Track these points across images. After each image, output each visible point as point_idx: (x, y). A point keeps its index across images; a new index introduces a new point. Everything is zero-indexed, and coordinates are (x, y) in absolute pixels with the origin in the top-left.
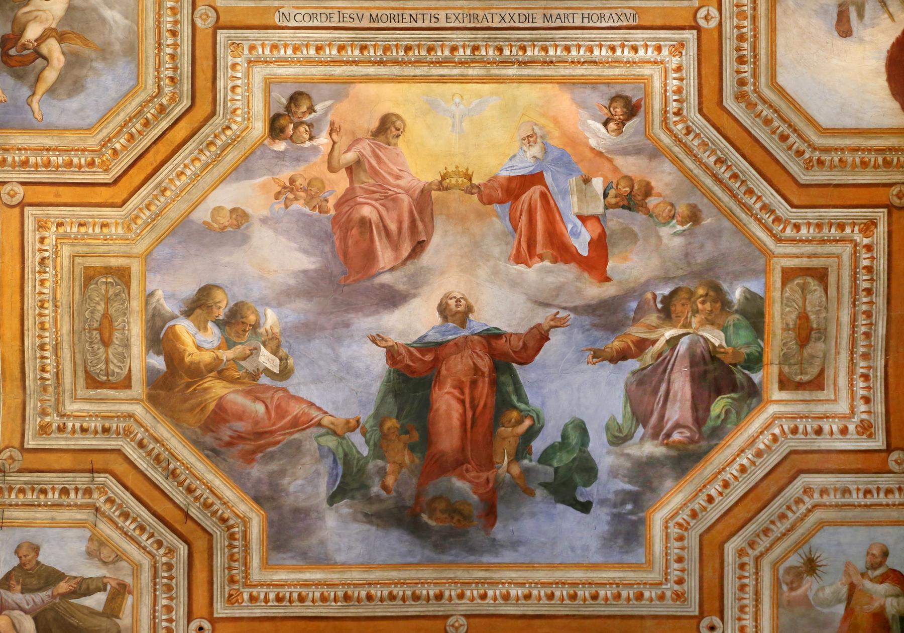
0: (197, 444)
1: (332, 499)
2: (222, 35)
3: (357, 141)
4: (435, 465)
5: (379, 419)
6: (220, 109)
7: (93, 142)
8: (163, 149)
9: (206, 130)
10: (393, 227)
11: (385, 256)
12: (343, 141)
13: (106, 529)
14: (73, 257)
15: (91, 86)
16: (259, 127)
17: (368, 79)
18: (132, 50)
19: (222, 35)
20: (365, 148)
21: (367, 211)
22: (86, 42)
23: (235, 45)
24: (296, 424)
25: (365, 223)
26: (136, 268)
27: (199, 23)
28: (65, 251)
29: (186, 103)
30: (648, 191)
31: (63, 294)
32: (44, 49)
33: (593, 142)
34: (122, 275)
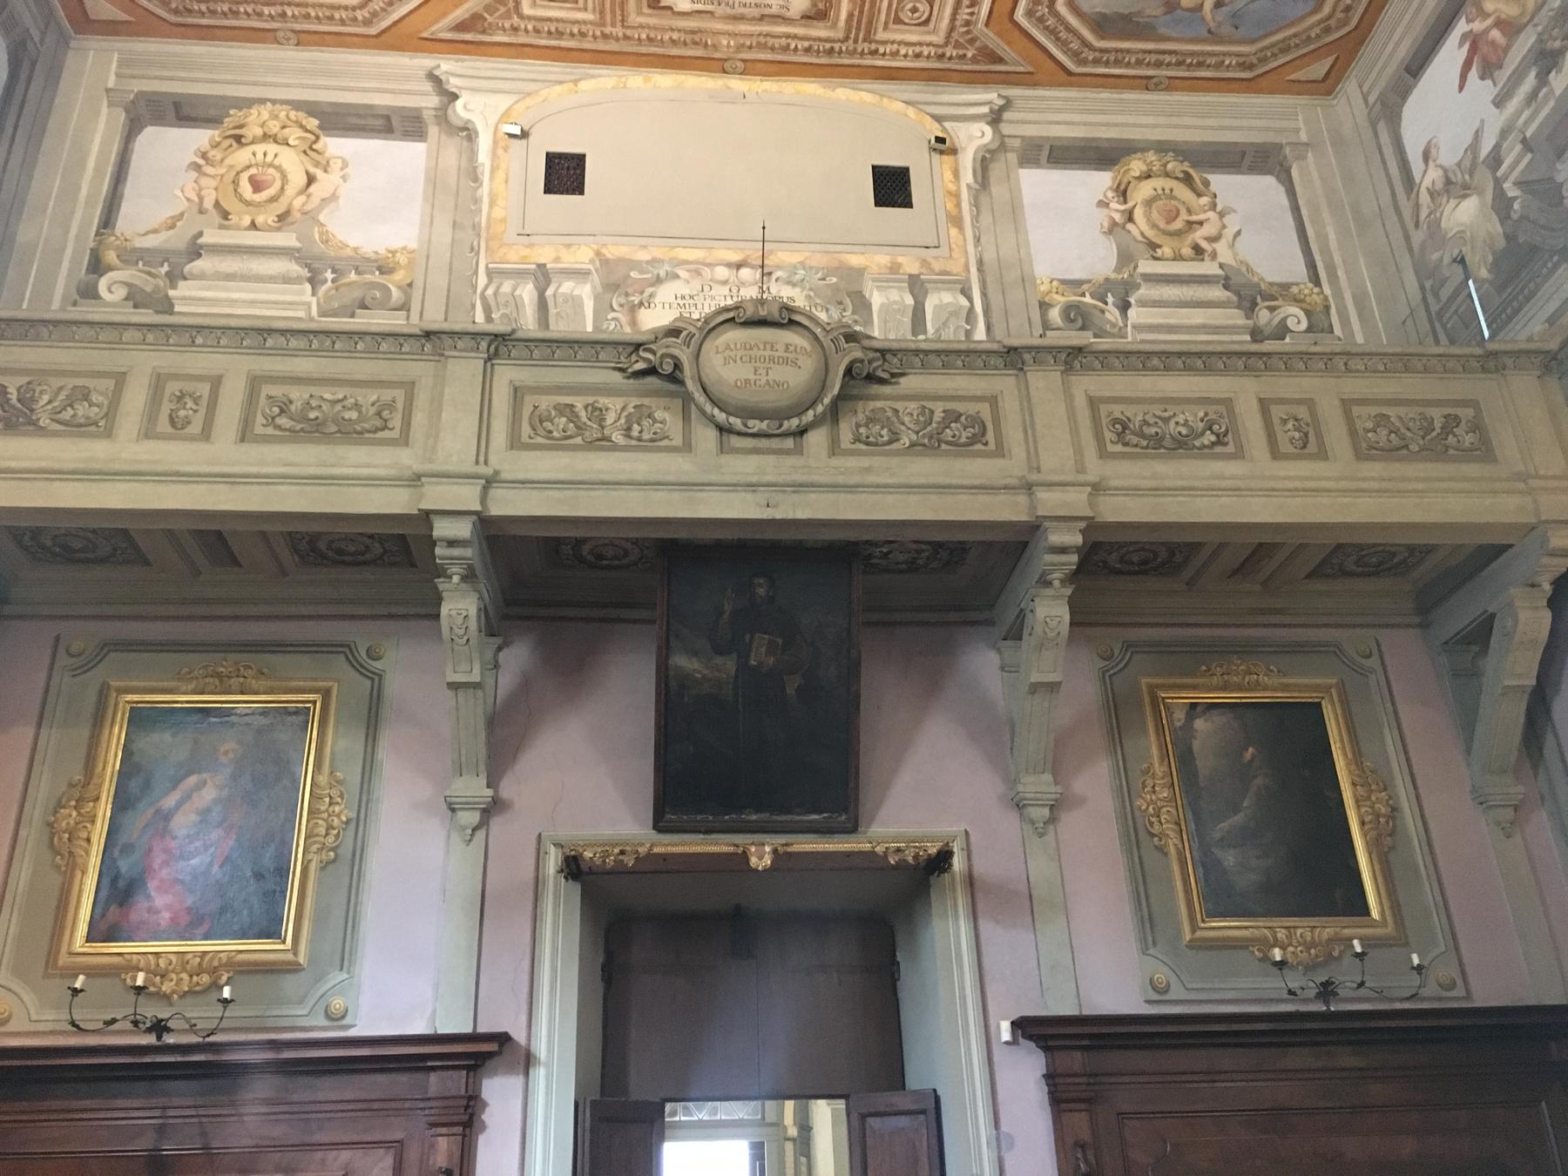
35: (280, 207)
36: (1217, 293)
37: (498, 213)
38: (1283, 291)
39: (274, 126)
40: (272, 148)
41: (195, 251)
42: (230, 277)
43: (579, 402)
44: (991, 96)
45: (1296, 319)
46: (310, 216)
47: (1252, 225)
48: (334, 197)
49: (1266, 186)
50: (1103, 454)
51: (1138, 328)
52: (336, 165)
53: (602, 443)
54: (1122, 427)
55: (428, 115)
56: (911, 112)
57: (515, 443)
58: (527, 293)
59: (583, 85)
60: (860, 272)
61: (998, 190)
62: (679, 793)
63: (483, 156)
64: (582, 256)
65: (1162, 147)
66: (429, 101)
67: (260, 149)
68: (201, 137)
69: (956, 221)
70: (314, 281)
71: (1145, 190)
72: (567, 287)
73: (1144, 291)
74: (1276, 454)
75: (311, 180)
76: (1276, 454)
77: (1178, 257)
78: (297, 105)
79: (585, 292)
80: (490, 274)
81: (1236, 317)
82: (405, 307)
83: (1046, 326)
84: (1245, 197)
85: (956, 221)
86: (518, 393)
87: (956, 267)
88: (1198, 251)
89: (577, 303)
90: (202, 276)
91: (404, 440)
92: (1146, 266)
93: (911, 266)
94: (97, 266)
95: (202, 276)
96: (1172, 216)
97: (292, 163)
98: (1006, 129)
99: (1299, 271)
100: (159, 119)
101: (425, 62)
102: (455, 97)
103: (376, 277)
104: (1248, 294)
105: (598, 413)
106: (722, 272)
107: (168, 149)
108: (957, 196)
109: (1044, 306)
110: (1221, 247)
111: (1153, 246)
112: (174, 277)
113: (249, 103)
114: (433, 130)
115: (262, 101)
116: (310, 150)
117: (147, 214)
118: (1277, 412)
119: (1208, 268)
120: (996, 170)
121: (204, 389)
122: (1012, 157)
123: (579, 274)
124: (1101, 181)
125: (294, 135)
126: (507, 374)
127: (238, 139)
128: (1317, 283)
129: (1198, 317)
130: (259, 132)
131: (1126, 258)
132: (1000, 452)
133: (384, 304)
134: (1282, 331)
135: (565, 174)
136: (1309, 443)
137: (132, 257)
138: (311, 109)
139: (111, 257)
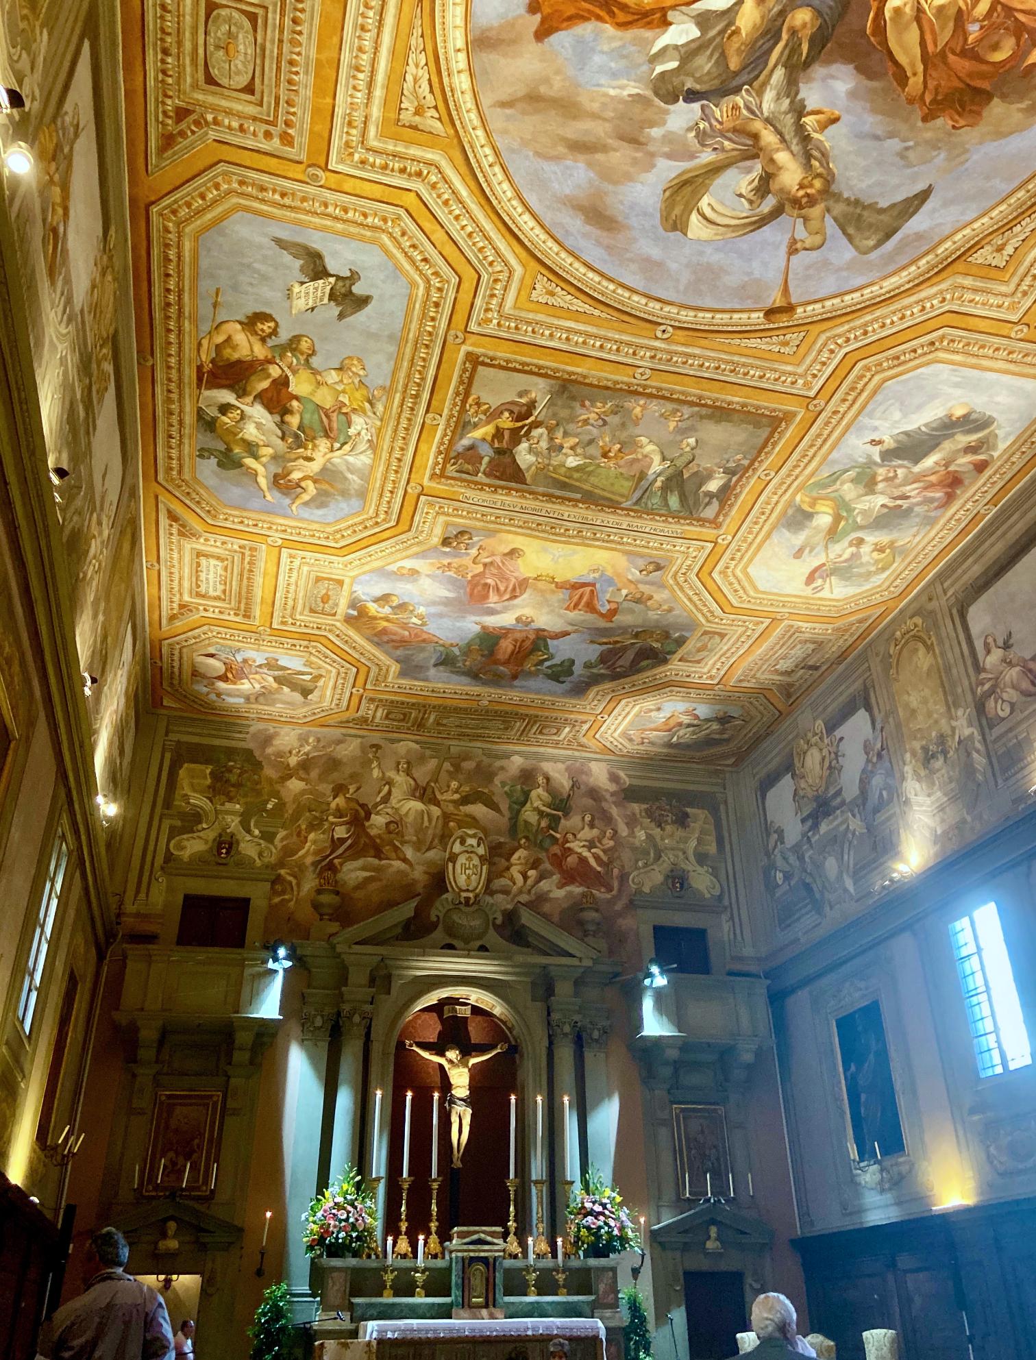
0: (372, 641)
1: (435, 665)
2: (423, 498)
3: (493, 555)
4: (497, 662)
5: (469, 645)
6: (414, 529)
7: (330, 530)
8: (373, 539)
9: (403, 536)
10: (502, 589)
11: (493, 597)
12: (484, 554)
13: (313, 659)
14: (309, 572)
15: (332, 505)
16: (436, 540)
17: (509, 532)
18: (362, 494)
19: (423, 498)
20: (498, 559)
21: (489, 581)
22: (332, 486)
23: (431, 504)
24: (424, 641)
25: (487, 586)
26: (347, 581)
27: (409, 490)
28: (305, 569)
29: (393, 523)
30: (650, 598)
31: (302, 583)
32: (303, 484)
33: (630, 577)
34: (340, 583)
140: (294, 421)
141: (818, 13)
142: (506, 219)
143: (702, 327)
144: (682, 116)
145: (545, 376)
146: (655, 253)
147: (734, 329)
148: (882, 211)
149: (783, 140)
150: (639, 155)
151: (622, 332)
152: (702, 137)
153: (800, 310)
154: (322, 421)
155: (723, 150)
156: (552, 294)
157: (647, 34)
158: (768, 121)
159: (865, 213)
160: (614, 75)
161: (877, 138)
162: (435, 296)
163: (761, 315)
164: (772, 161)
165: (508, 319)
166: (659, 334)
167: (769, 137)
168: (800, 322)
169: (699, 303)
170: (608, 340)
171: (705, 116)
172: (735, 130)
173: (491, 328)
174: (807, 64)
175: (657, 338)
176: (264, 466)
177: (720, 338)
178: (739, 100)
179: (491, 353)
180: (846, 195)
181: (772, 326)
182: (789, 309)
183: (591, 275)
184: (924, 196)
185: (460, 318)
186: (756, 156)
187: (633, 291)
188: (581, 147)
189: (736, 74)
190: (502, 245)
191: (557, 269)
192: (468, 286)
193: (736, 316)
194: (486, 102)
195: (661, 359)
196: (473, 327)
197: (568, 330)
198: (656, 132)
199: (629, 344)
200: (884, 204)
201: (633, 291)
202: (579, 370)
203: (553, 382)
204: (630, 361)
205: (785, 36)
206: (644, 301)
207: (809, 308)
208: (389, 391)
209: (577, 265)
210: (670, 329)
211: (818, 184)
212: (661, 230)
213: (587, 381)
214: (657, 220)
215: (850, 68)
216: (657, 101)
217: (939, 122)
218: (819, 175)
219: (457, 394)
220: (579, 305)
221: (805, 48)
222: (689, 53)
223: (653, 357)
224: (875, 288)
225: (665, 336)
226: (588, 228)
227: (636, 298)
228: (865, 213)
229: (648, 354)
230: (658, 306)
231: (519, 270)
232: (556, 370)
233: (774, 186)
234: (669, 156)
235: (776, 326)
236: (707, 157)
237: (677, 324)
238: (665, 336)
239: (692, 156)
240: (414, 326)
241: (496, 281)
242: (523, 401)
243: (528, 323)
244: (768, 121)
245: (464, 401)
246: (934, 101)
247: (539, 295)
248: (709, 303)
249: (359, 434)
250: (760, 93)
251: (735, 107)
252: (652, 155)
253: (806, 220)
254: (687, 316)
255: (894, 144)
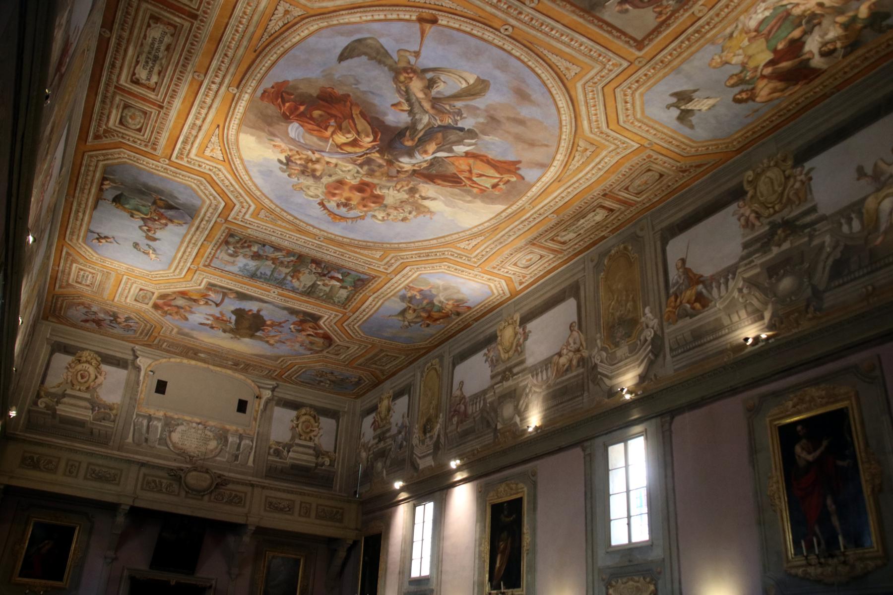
35: (87, 385)
36: (311, 451)
37: (142, 396)
38: (326, 454)
39: (89, 358)
40: (87, 365)
41: (64, 395)
42: (72, 405)
43: (157, 480)
44: (274, 383)
45: (327, 461)
46: (95, 389)
47: (325, 433)
48: (100, 385)
49: (333, 422)
50: (265, 510)
51: (291, 458)
52: (103, 373)
53: (160, 491)
54: (271, 503)
55: (130, 362)
56: (253, 384)
57: (142, 489)
58: (145, 422)
59: (172, 360)
60: (228, 431)
61: (268, 412)
62: (156, 563)
63: (141, 378)
64: (161, 414)
65: (311, 406)
66: (130, 358)
67: (85, 365)
68: (70, 358)
69: (255, 419)
70: (93, 410)
71: (303, 419)
72: (155, 423)
73: (295, 448)
74: (300, 515)
75: (96, 377)
76: (300, 515)
77: (305, 440)
78: (97, 353)
79: (160, 425)
80: (138, 415)
81: (313, 459)
82: (114, 421)
83: (269, 454)
84: (327, 424)
85: (255, 419)
86: (145, 475)
87: (252, 433)
88: (311, 438)
89: (157, 427)
90: (65, 403)
91: (118, 484)
92: (297, 441)
93: (241, 431)
94: (39, 396)
95: (65, 403)
96: (307, 428)
97: (92, 370)
98: (275, 394)
99: (331, 449)
100: (60, 351)
101: (133, 345)
102: (137, 357)
103: (107, 411)
104: (318, 452)
105: (161, 483)
106: (194, 425)
107: (62, 360)
108: (257, 411)
109: (270, 448)
110: (316, 439)
111: (301, 435)
112: (58, 403)
113: (83, 349)
114: (130, 367)
115: (87, 349)
116: (97, 368)
117: (54, 381)
118: (303, 505)
119: (311, 444)
120: (269, 405)
121: (77, 464)
122: (274, 402)
123: (158, 419)
124: (293, 413)
125: (94, 362)
126: (144, 470)
127: (79, 361)
128: (335, 452)
129: (305, 457)
130: (85, 359)
131: (293, 438)
132: (244, 506)
133: (108, 420)
134: (323, 464)
135: (161, 387)
136: (307, 514)
137: (48, 394)
138: (99, 353)
139: (42, 393)
140: (796, 33)
141: (402, 143)
142: (571, 107)
143: (480, 25)
144: (468, 123)
145: (600, 20)
146: (497, 73)
147: (459, 18)
148: (365, 54)
149: (420, 103)
150: (492, 112)
151: (534, 37)
152: (459, 113)
153: (414, 18)
154: (779, 27)
155: (450, 105)
156: (567, 69)
157: (475, 151)
158: (427, 112)
159: (375, 55)
160: (493, 144)
161: (373, 93)
162: (634, 86)
163: (440, 22)
164: (426, 94)
165: (602, 62)
166: (510, 29)
167: (427, 106)
168: (414, 9)
169: (480, 42)
170: (546, 34)
171: (456, 122)
172: (443, 113)
173: (616, 59)
174: (407, 128)
175: (513, 27)
176: (858, 9)
177: (470, 13)
178: (439, 123)
179: (626, 46)
180: (386, 68)
181: (434, 12)
182: (421, 20)
183: (539, 72)
184: (342, 57)
185: (629, 72)
186: (434, 98)
187: (518, 58)
188: (521, 122)
189: (440, 131)
190: (581, 97)
191: (556, 78)
192: (613, 85)
193: (457, 26)
194: (554, 149)
195: (515, 10)
196: (625, 64)
197: (569, 46)
198: (481, 120)
199: (533, 27)
200: (364, 58)
201: (518, 58)
202: (575, 17)
203: (598, 14)
204: (537, 15)
205: (416, 139)
206: (513, 52)
207: (407, 17)
208: (712, 41)
209: (545, 78)
210: (502, 30)
211: (402, 78)
212: (491, 82)
213: (573, 8)
214: (492, 86)
215: (387, 123)
216: (477, 132)
217: (341, 92)
218: (402, 82)
219: (669, 26)
220: (554, 59)
221: (408, 134)
222: (459, 142)
223: (520, 13)
224: (364, 18)
225: (506, 27)
226: (530, 93)
227: (518, 54)
228: (375, 55)
229: (523, 16)
230: (505, 47)
231: (579, 85)
232: (592, 22)
233: (426, 83)
234: (478, 109)
235: (431, 11)
236: (459, 104)
237: (497, 33)
238: (506, 27)
239: (467, 106)
240: (657, 77)
241: (595, 83)
242: (627, 6)
243: (591, 57)
244: (427, 112)
245: (669, 18)
246: (345, 102)
247: (575, 69)
248: (474, 41)
249: (765, 9)
250: (429, 123)
251: (442, 121)
252: (486, 111)
253: (409, 63)
254: (489, 35)
255: (363, 88)
